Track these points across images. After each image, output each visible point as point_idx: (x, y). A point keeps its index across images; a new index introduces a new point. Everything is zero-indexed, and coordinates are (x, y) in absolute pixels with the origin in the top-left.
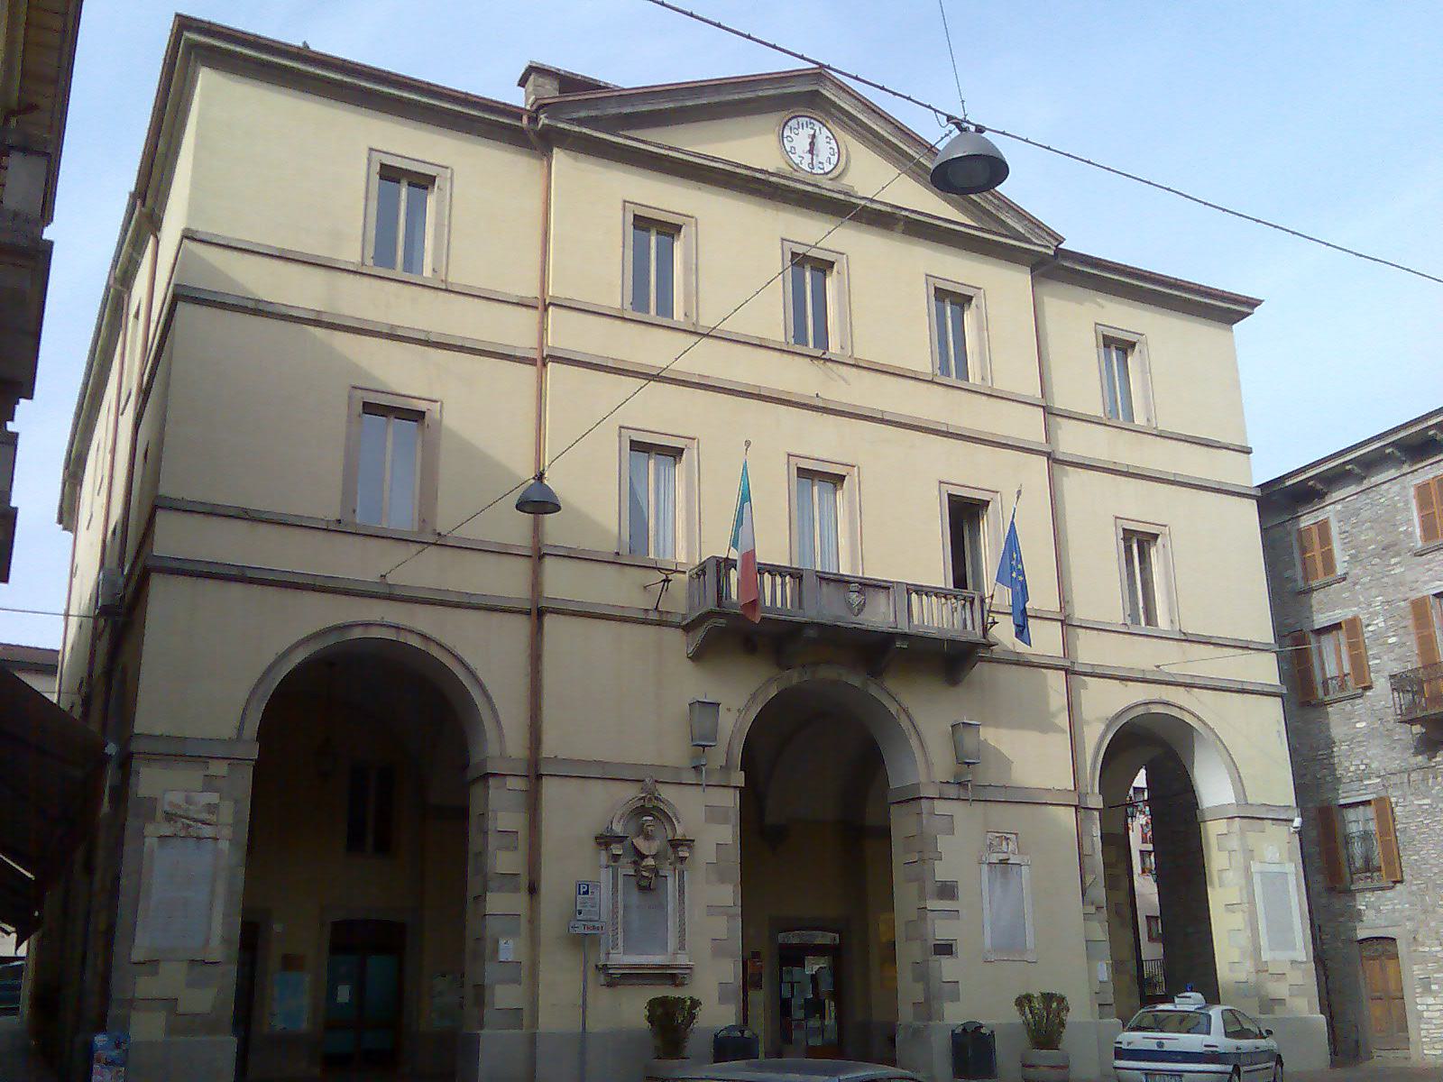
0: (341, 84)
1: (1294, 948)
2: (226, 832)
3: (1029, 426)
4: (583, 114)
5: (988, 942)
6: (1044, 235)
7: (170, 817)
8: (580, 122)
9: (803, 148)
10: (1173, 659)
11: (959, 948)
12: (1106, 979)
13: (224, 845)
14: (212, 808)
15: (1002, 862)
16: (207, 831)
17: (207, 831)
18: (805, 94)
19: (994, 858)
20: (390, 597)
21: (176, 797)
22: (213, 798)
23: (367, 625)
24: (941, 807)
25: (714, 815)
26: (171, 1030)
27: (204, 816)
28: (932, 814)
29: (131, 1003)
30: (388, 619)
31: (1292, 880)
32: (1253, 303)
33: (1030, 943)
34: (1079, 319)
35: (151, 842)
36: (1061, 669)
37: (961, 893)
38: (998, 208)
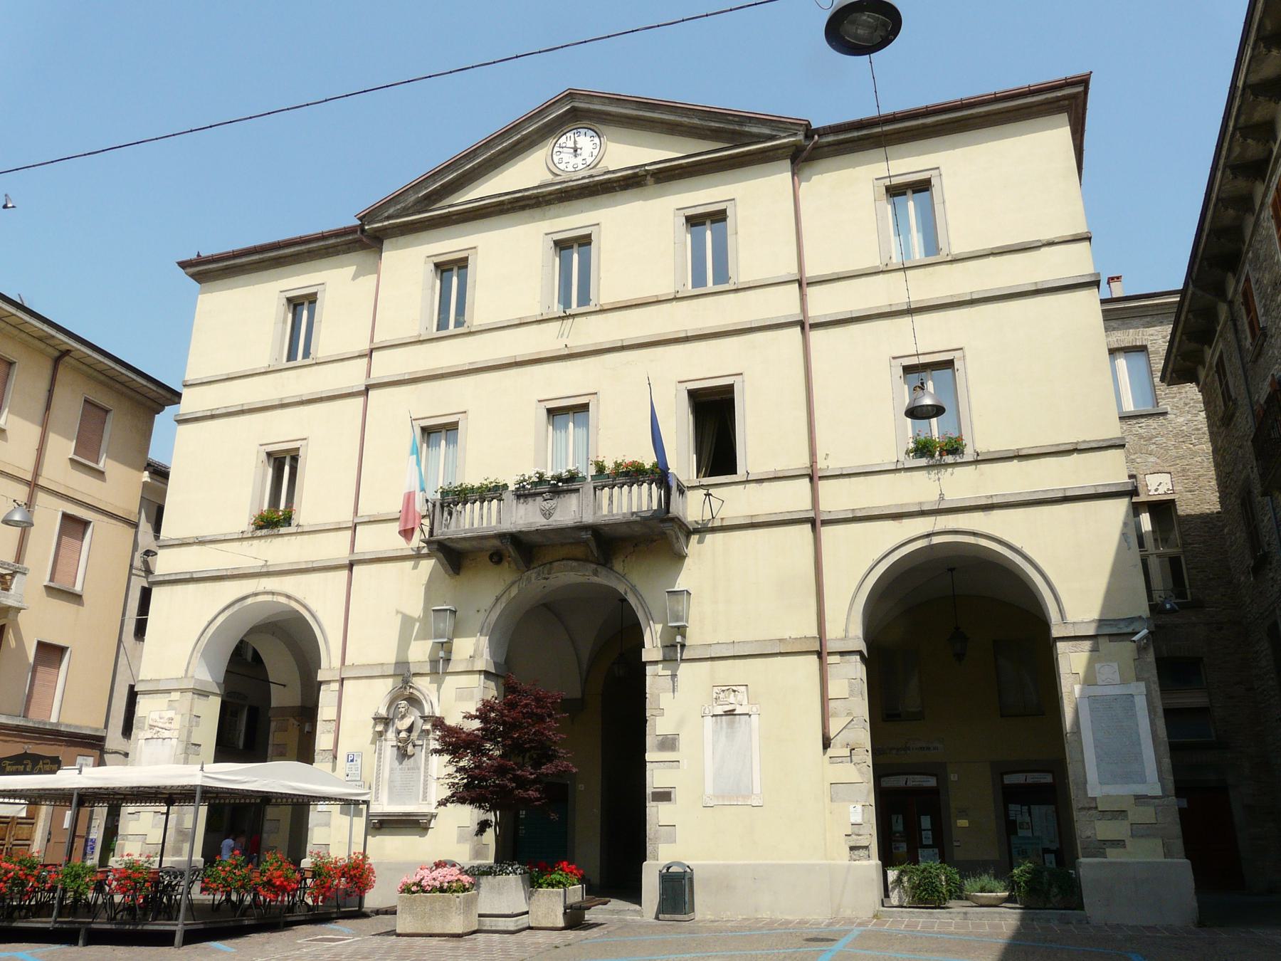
0: (262, 261)
1: (1143, 781)
2: (176, 734)
5: (709, 790)
7: (152, 727)
8: (388, 218)
11: (678, 795)
13: (174, 741)
16: (166, 734)
17: (166, 734)
19: (719, 710)
21: (154, 716)
22: (171, 714)
23: (256, 594)
27: (167, 726)
30: (269, 588)
31: (1141, 703)
32: (1084, 81)
33: (757, 789)
34: (851, 187)
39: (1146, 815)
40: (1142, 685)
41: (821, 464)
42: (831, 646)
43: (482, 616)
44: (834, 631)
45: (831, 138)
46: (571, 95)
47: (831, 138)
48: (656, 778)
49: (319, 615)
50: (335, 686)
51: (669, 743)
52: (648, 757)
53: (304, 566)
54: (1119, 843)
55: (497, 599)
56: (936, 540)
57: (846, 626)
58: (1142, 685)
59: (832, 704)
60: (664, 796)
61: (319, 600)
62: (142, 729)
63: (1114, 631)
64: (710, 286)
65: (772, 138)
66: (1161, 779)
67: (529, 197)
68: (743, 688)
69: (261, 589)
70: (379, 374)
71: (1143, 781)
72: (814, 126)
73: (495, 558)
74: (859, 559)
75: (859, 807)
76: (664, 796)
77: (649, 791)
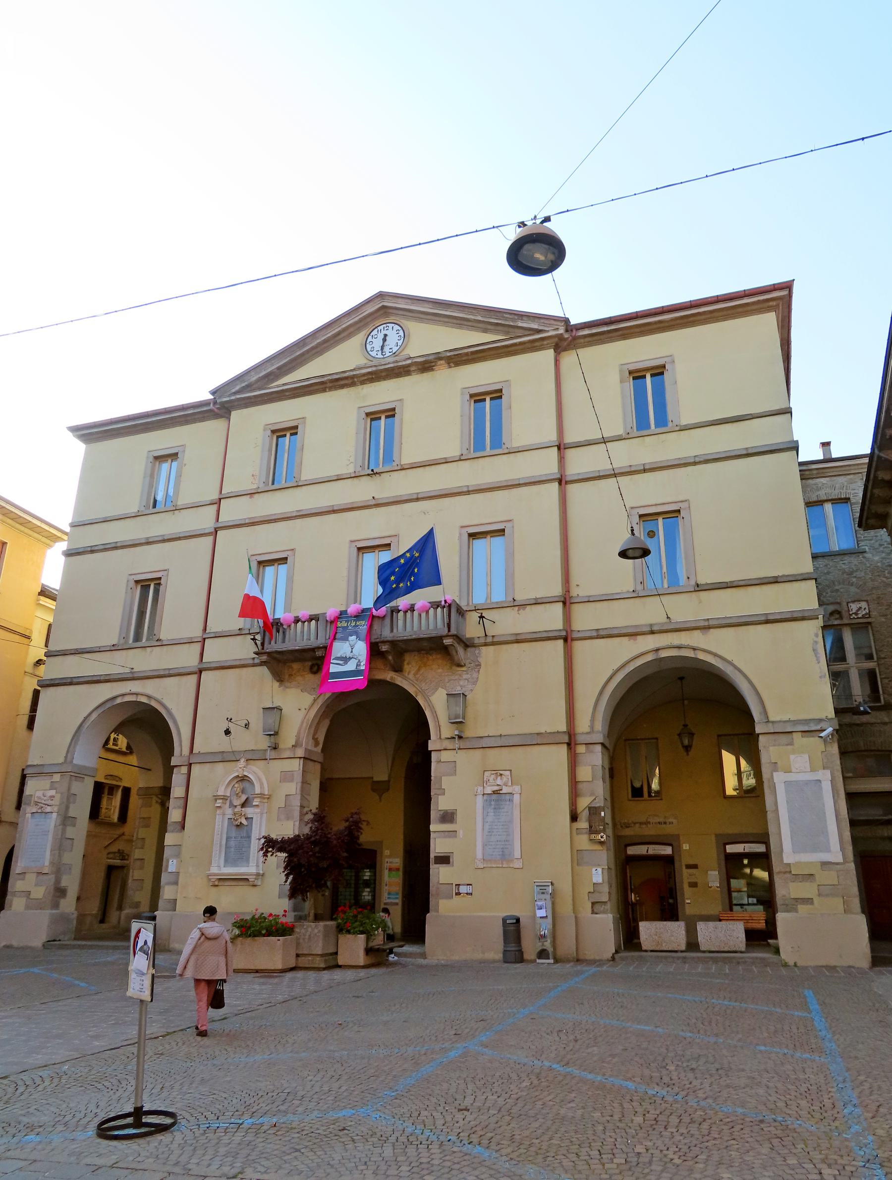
1: (828, 850)
2: (56, 809)
3: (548, 464)
4: (238, 388)
5: (479, 855)
6: (553, 322)
7: (36, 803)
8: (235, 393)
9: (388, 341)
10: (684, 608)
11: (455, 859)
12: (600, 881)
13: (54, 815)
14: (52, 797)
15: (494, 792)
16: (49, 809)
18: (382, 309)
19: (489, 790)
20: (133, 679)
21: (39, 794)
22: (53, 793)
23: (123, 695)
24: (445, 756)
25: (286, 777)
26: (27, 907)
27: (50, 802)
28: (439, 762)
29: (14, 894)
30: (134, 690)
31: (827, 786)
32: (788, 286)
33: (517, 854)
34: (603, 369)
35: (29, 815)
36: (556, 638)
37: (459, 817)
38: (513, 320)
39: (829, 878)
40: (828, 773)
41: (574, 592)
42: (580, 739)
43: (303, 712)
44: (583, 725)
45: (586, 332)
46: (381, 295)
47: (586, 332)
48: (438, 846)
49: (174, 712)
50: (184, 770)
51: (448, 817)
52: (433, 827)
53: (162, 673)
54: (809, 901)
55: (315, 700)
56: (664, 654)
57: (592, 721)
58: (828, 773)
59: (580, 786)
60: (444, 860)
61: (173, 700)
62: (29, 804)
63: (806, 728)
64: (488, 451)
65: (539, 331)
66: (842, 849)
67: (346, 378)
68: (508, 773)
69: (128, 691)
70: (224, 518)
71: (828, 850)
72: (573, 322)
73: (315, 668)
74: (604, 667)
75: (600, 870)
76: (444, 860)
77: (432, 856)
